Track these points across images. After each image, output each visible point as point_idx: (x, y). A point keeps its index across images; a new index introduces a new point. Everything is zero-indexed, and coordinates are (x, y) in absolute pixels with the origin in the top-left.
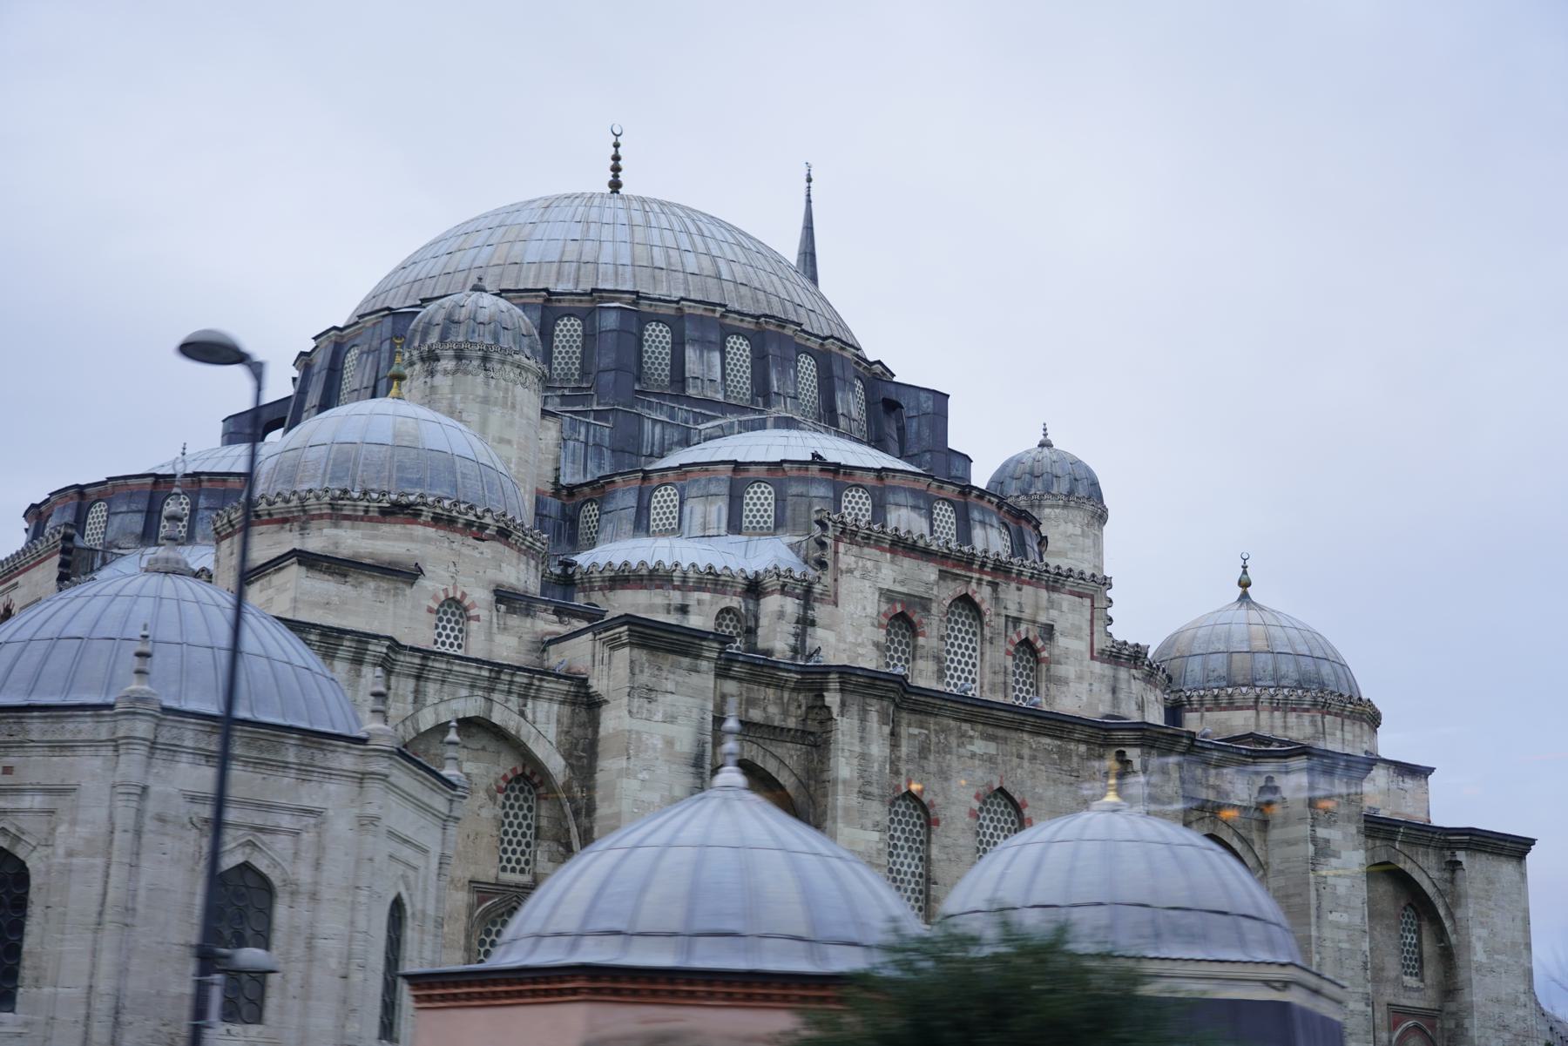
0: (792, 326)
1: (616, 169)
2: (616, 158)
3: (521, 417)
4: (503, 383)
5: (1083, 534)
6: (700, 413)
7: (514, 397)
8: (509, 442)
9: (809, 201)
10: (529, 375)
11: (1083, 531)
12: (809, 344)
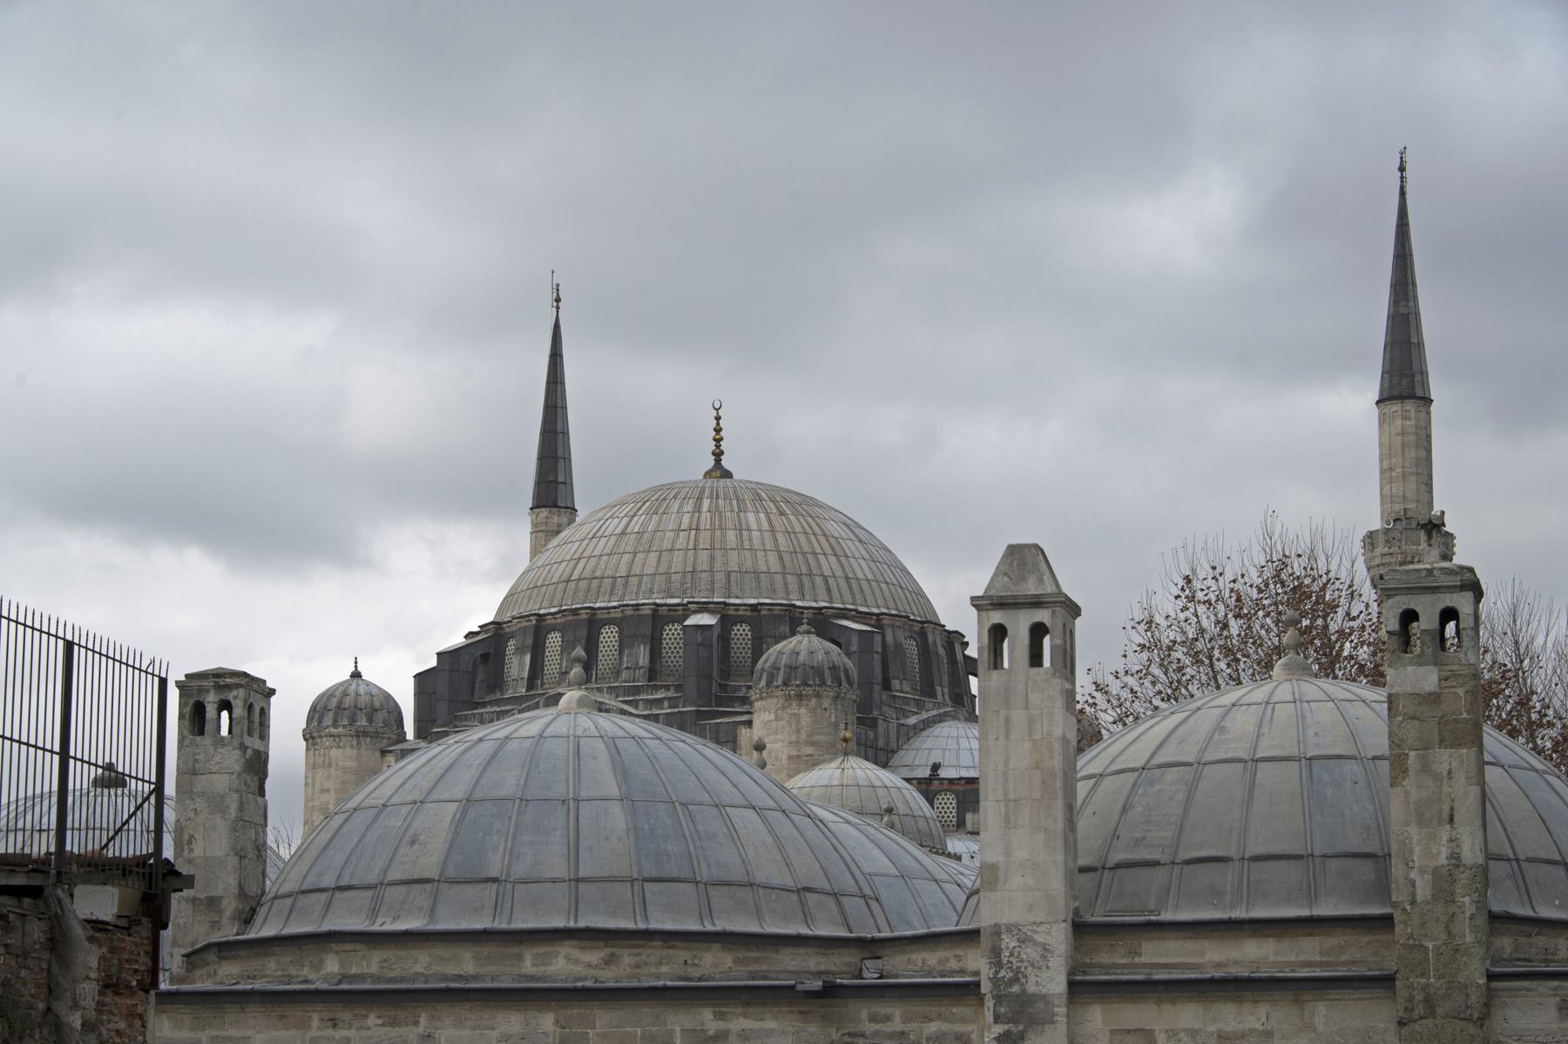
1: (718, 441)
2: (718, 430)
3: (336, 770)
4: (322, 750)
5: (777, 718)
6: (501, 711)
7: (330, 758)
9: (1403, 194)
10: (343, 738)
11: (777, 716)
12: (612, 615)
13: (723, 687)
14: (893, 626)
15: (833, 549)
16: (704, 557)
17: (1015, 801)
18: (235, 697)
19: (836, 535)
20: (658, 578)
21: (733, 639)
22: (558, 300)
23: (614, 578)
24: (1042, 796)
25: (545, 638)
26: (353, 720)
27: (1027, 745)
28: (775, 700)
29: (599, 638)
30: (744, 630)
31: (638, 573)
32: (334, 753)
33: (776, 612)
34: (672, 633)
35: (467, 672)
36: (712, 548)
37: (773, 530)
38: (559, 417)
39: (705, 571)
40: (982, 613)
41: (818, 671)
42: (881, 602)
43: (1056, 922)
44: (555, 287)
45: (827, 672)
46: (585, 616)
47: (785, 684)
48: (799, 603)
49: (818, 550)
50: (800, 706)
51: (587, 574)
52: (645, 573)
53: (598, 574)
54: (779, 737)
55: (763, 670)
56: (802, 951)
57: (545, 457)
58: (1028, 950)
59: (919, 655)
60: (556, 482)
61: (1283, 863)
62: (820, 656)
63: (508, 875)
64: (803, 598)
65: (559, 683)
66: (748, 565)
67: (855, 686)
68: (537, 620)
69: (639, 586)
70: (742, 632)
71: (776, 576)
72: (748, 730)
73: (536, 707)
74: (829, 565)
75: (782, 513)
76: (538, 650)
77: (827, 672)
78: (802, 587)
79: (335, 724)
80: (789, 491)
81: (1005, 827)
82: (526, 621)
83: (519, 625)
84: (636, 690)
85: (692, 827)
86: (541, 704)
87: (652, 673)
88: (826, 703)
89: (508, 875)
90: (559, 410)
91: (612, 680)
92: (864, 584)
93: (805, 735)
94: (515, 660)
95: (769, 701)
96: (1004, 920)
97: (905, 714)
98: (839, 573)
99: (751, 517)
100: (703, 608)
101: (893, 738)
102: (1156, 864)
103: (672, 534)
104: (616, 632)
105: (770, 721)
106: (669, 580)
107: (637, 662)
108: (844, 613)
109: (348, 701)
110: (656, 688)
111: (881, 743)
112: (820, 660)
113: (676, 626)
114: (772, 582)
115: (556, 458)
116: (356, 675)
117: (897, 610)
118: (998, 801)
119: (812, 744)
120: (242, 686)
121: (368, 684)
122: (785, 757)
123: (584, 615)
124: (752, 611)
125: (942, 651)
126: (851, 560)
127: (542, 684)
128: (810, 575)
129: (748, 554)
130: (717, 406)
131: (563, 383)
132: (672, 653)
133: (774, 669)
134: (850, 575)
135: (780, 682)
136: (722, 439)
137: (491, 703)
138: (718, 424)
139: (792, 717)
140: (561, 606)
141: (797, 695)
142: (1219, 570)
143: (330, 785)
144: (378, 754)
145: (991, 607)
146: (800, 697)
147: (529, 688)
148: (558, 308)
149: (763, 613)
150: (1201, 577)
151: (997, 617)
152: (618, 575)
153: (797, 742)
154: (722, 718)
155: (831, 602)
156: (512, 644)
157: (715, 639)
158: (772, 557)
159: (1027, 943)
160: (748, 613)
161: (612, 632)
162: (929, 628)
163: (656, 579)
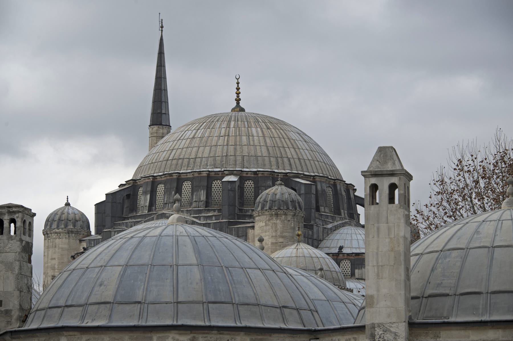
0: (174, 175)
1: (238, 94)
2: (238, 89)
3: (58, 249)
4: (52, 240)
5: (266, 225)
6: (136, 221)
7: (55, 243)
8: (54, 259)
10: (61, 234)
12: (188, 176)
13: (241, 210)
14: (321, 182)
15: (292, 145)
16: (231, 148)
17: (382, 266)
18: (17, 217)
19: (294, 138)
20: (210, 159)
21: (245, 188)
22: (162, 27)
23: (189, 159)
24: (394, 264)
25: (157, 187)
26: (66, 226)
27: (387, 240)
28: (265, 216)
29: (182, 187)
30: (250, 183)
31: (200, 157)
32: (58, 241)
33: (266, 175)
34: (216, 185)
35: (120, 203)
36: (236, 145)
37: (264, 136)
38: (163, 83)
39: (232, 156)
40: (366, 179)
41: (285, 203)
42: (315, 170)
43: (401, 322)
44: (160, 21)
45: (290, 203)
46: (175, 177)
47: (270, 209)
48: (276, 171)
49: (285, 146)
50: (277, 219)
51: (176, 157)
52: (204, 156)
53: (182, 157)
54: (267, 234)
55: (259, 202)
56: (282, 335)
57: (155, 102)
58: (388, 335)
59: (333, 195)
60: (161, 113)
61: (506, 295)
62: (286, 196)
63: (145, 300)
64: (278, 168)
65: (163, 208)
66: (252, 153)
67: (303, 210)
68: (153, 179)
69: (201, 163)
70: (249, 185)
71: (266, 158)
72: (252, 230)
73: (152, 219)
74: (290, 153)
75: (268, 128)
76: (153, 193)
77: (290, 203)
78: (278, 163)
79: (58, 228)
80: (272, 118)
81: (377, 278)
82: (147, 179)
83: (145, 181)
84: (200, 212)
85: (231, 278)
86: (155, 218)
87: (207, 204)
88: (289, 218)
89: (145, 300)
90: (163, 79)
91: (188, 207)
92: (307, 162)
93: (279, 233)
94: (143, 198)
95: (262, 217)
96: (376, 322)
97: (327, 223)
98: (295, 156)
99: (254, 130)
100: (231, 173)
101: (321, 234)
102: (447, 295)
103: (216, 138)
104: (190, 184)
105: (262, 226)
106: (215, 160)
107: (200, 198)
108: (297, 176)
109: (64, 217)
110: (209, 211)
111: (315, 236)
112: (287, 197)
113: (218, 182)
114: (264, 161)
115: (161, 102)
116: (68, 204)
117: (323, 174)
118: (374, 266)
119: (283, 237)
120: (20, 212)
121: (73, 208)
122: (270, 243)
123: (175, 176)
124: (254, 174)
125: (344, 193)
126: (301, 150)
127: (155, 209)
128: (282, 157)
129: (252, 147)
130: (238, 78)
131: (164, 66)
132: (217, 194)
133: (265, 202)
134: (301, 158)
135: (267, 208)
136: (240, 93)
137: (131, 218)
138: (238, 86)
139: (274, 224)
140: (164, 172)
141: (275, 214)
142: (474, 156)
143: (56, 256)
144: (78, 241)
145: (370, 176)
146: (277, 215)
147: (150, 210)
148: (162, 31)
149: (259, 175)
150: (466, 160)
151: (373, 181)
152: (191, 157)
153: (276, 236)
154: (240, 224)
155: (291, 170)
156: (141, 190)
157: (237, 188)
158: (264, 149)
159: (387, 332)
160: (253, 175)
161: (188, 184)
162: (338, 182)
163: (209, 159)
